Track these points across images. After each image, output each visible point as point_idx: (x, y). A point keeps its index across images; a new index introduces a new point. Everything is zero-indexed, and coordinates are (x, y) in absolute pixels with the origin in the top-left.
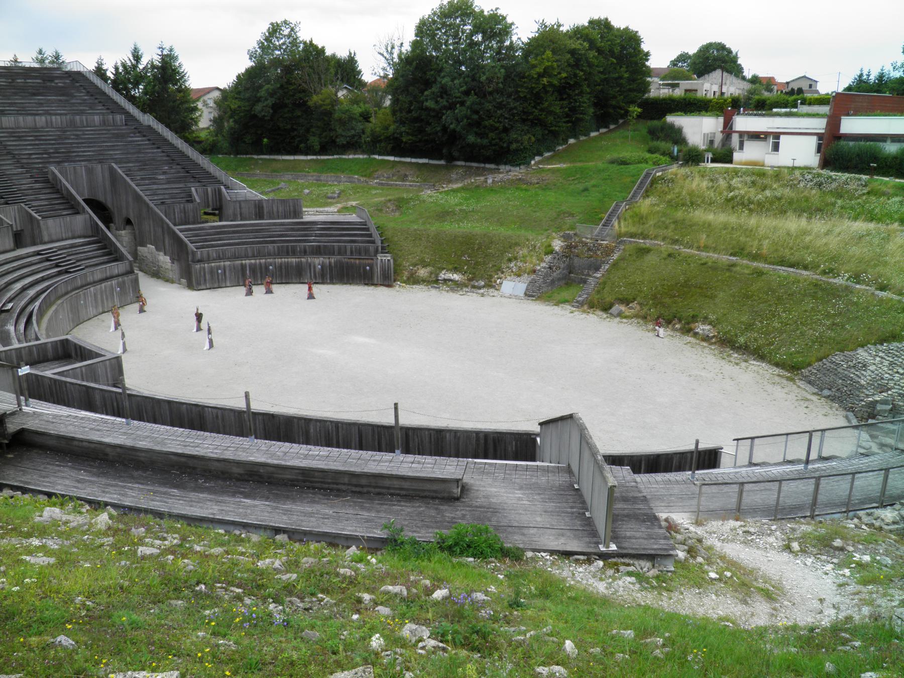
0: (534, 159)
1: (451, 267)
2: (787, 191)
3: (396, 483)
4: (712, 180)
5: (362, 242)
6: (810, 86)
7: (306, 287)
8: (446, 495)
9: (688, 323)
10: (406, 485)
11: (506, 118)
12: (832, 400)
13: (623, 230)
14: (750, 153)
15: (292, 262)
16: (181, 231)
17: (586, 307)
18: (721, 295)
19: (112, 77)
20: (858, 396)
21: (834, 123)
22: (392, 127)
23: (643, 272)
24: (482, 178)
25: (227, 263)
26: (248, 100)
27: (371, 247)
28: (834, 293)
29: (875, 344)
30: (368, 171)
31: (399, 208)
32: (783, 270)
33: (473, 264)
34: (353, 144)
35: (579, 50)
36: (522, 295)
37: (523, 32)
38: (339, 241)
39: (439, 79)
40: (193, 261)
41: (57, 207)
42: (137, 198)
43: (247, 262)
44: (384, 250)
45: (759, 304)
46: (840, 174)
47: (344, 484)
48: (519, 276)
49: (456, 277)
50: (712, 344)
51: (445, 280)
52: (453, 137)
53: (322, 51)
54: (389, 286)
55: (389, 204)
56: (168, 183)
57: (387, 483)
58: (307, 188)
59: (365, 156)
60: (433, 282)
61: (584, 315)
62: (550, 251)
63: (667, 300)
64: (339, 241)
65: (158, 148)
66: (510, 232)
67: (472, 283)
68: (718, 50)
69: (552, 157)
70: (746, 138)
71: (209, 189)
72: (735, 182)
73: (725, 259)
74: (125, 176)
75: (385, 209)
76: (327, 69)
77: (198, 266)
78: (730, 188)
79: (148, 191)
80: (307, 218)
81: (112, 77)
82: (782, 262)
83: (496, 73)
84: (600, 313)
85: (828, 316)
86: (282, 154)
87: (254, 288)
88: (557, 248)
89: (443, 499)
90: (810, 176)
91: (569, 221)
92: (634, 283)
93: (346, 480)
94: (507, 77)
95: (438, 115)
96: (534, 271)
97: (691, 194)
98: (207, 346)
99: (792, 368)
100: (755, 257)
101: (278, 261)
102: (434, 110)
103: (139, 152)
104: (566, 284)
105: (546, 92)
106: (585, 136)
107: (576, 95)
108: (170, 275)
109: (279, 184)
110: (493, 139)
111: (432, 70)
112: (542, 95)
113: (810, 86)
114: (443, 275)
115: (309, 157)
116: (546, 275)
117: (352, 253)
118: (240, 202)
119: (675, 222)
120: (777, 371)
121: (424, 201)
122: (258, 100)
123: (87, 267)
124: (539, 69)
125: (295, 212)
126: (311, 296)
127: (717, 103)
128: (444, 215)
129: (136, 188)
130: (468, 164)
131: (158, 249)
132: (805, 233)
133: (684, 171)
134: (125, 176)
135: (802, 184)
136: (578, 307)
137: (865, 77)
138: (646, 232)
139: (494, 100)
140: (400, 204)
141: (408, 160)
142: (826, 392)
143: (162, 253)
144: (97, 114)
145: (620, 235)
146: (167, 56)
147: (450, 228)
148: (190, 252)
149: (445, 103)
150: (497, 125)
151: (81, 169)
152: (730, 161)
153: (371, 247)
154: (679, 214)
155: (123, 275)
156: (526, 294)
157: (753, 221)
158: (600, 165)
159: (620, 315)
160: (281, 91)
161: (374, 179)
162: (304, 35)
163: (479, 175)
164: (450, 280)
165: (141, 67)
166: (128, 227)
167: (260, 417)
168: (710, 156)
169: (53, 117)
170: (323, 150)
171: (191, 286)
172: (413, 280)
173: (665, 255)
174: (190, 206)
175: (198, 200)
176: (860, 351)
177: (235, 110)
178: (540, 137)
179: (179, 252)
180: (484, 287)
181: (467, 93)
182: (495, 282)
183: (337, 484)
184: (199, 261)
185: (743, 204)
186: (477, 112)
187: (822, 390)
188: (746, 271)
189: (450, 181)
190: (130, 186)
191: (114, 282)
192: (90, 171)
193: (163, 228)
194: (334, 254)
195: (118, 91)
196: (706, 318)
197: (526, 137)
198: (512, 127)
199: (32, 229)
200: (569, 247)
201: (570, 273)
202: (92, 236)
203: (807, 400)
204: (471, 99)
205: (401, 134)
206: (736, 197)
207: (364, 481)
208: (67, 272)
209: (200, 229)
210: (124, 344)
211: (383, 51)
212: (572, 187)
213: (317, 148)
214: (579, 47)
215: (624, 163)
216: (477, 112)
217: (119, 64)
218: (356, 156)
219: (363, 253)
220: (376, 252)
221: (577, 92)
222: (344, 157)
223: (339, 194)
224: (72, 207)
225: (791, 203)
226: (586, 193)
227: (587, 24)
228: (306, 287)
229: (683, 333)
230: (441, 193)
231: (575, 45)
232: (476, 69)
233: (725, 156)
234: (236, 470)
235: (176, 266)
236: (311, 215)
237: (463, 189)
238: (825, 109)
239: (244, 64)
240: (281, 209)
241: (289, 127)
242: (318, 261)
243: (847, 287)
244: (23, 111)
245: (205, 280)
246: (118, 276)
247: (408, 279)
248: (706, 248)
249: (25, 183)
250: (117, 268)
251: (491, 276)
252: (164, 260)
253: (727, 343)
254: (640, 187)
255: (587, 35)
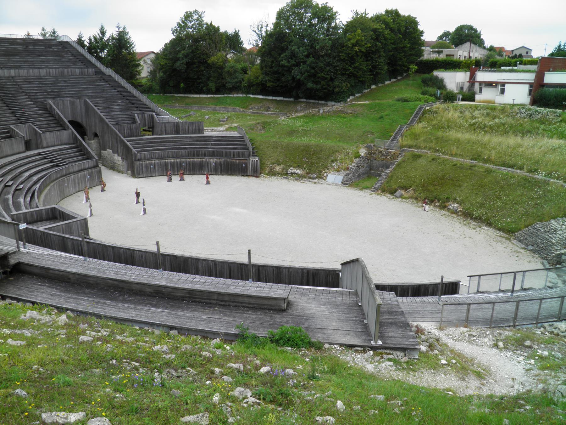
0: (349, 98)
1: (295, 165)
2: (510, 120)
3: (246, 300)
4: (461, 112)
5: (241, 149)
6: (527, 53)
7: (205, 177)
8: (277, 308)
9: (444, 203)
10: (252, 301)
11: (332, 72)
12: (534, 252)
13: (404, 143)
14: (485, 96)
15: (197, 161)
16: (128, 141)
17: (380, 191)
18: (465, 184)
19: (88, 45)
20: (550, 250)
21: (540, 76)
22: (260, 78)
23: (416, 169)
24: (317, 110)
25: (157, 161)
26: (172, 59)
27: (246, 152)
28: (536, 184)
29: (562, 217)
30: (245, 105)
31: (264, 128)
32: (504, 170)
33: (310, 164)
34: (236, 88)
35: (379, 29)
36: (340, 183)
37: (343, 17)
38: (226, 148)
39: (290, 47)
40: (135, 160)
41: (52, 125)
42: (102, 120)
43: (169, 160)
44: (254, 154)
45: (489, 191)
46: (543, 109)
47: (214, 300)
48: (338, 171)
49: (299, 171)
50: (458, 216)
51: (292, 173)
52: (299, 84)
53: (218, 29)
54: (257, 177)
55: (258, 126)
56: (121, 111)
57: (241, 299)
58: (207, 115)
59: (244, 95)
60: (285, 174)
61: (379, 197)
62: (358, 156)
63: (431, 188)
64: (226, 148)
65: (115, 89)
66: (333, 144)
67: (309, 175)
68: (468, 30)
69: (360, 97)
70: (483, 86)
71: (146, 115)
72: (476, 113)
73: (468, 162)
74: (94, 107)
75: (255, 129)
76: (221, 41)
77: (138, 163)
78: (473, 117)
79: (108, 116)
80: (206, 134)
81: (88, 45)
82: (504, 165)
83: (325, 44)
84: (389, 195)
85: (532, 199)
86: (192, 94)
87: (173, 177)
88: (362, 154)
89: (275, 310)
90: (524, 110)
91: (370, 137)
92: (410, 177)
93: (215, 297)
94: (333, 46)
95: (289, 70)
96: (348, 169)
97: (448, 121)
98: (142, 213)
99: (509, 232)
100: (486, 161)
101: (188, 160)
102: (287, 67)
103: (103, 92)
104: (368, 177)
105: (358, 56)
106: (382, 83)
107: (376, 58)
108: (121, 168)
109: (190, 112)
110: (324, 85)
111: (285, 42)
112: (355, 57)
113: (527, 53)
114: (291, 170)
115: (209, 96)
116: (355, 171)
117: (234, 156)
118: (165, 123)
119: (437, 139)
120: (499, 233)
121: (280, 124)
122: (178, 59)
123: (69, 163)
124: (353, 41)
125: (199, 130)
126: (208, 183)
127: (466, 63)
128: (292, 132)
129: (101, 114)
130: (308, 101)
131: (114, 152)
132: (519, 146)
133: (443, 106)
134: (94, 107)
135: (519, 115)
136: (375, 191)
137: (562, 47)
138: (418, 145)
139: (325, 60)
140: (265, 126)
141: (270, 98)
142: (530, 247)
143: (116, 155)
144: (78, 68)
145: (402, 146)
146: (122, 32)
147: (296, 141)
148: (133, 154)
149: (294, 62)
150: (327, 76)
151: (67, 101)
152: (473, 100)
153: (246, 152)
154: (440, 134)
155: (92, 168)
156: (342, 183)
157: (486, 138)
158: (391, 102)
159: (401, 196)
160: (192, 54)
161: (249, 109)
162: (207, 19)
163: (315, 108)
164: (295, 173)
165: (106, 39)
166: (96, 138)
167: (168, 257)
168: (461, 97)
169: (51, 70)
170: (218, 91)
171: (134, 175)
172: (272, 173)
173: (430, 159)
174: (134, 126)
175: (139, 122)
176: (553, 221)
177: (163, 65)
178: (353, 84)
179: (127, 154)
180: (316, 178)
181: (308, 56)
182: (323, 175)
183: (210, 299)
184: (139, 160)
185: (481, 127)
186: (314, 68)
187: (527, 246)
188: (481, 170)
189: (296, 112)
190: (97, 113)
191: (86, 172)
192: (73, 104)
193: (117, 139)
194: (223, 156)
195: (91, 53)
196: (455, 199)
197: (344, 84)
198: (336, 77)
199: (37, 139)
200: (370, 153)
201: (370, 170)
202: (73, 144)
203: (518, 252)
204: (311, 59)
205: (266, 81)
206: (476, 123)
207: (226, 298)
208: (57, 166)
209: (140, 140)
210: (91, 211)
211: (256, 29)
212: (373, 116)
213: (214, 89)
214: (379, 27)
215: (406, 101)
216: (314, 68)
217: (92, 37)
218: (238, 95)
219: (241, 156)
220: (249, 155)
221: (377, 56)
222: (230, 95)
223: (227, 119)
224: (61, 126)
225: (511, 127)
226: (381, 120)
227: (384, 13)
228: (205, 177)
229: (440, 209)
230: (290, 119)
231: (376, 26)
232: (314, 41)
233: (471, 98)
234: (148, 290)
235: (125, 163)
236: (210, 131)
237: (305, 116)
238: (534, 67)
239: (170, 37)
240: (190, 128)
241: (196, 77)
242: (213, 161)
243: (545, 181)
244: (32, 66)
245: (143, 172)
246: (89, 168)
247: (269, 172)
248: (456, 155)
249: (33, 110)
250: (88, 163)
251: (321, 171)
252: (118, 159)
253: (467, 215)
254: (415, 116)
255: (384, 20)
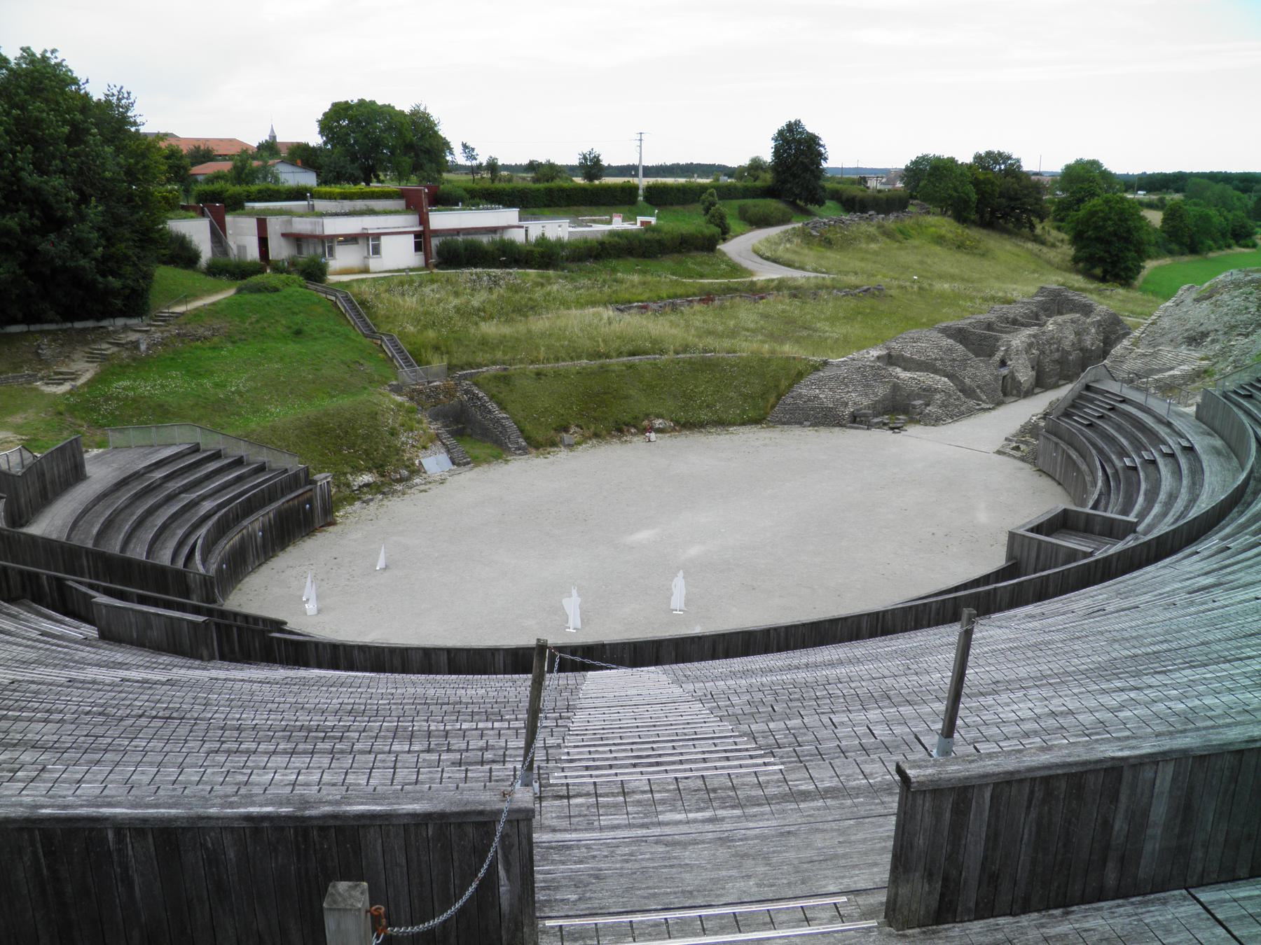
164: (367, 485)
242: (255, 524)
